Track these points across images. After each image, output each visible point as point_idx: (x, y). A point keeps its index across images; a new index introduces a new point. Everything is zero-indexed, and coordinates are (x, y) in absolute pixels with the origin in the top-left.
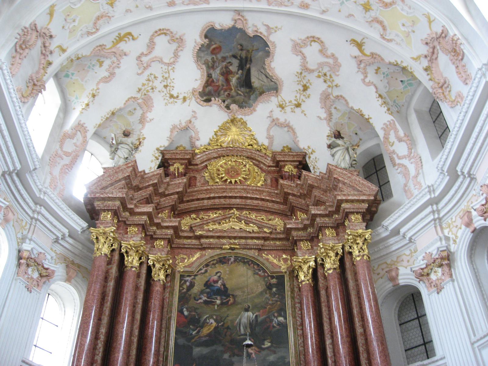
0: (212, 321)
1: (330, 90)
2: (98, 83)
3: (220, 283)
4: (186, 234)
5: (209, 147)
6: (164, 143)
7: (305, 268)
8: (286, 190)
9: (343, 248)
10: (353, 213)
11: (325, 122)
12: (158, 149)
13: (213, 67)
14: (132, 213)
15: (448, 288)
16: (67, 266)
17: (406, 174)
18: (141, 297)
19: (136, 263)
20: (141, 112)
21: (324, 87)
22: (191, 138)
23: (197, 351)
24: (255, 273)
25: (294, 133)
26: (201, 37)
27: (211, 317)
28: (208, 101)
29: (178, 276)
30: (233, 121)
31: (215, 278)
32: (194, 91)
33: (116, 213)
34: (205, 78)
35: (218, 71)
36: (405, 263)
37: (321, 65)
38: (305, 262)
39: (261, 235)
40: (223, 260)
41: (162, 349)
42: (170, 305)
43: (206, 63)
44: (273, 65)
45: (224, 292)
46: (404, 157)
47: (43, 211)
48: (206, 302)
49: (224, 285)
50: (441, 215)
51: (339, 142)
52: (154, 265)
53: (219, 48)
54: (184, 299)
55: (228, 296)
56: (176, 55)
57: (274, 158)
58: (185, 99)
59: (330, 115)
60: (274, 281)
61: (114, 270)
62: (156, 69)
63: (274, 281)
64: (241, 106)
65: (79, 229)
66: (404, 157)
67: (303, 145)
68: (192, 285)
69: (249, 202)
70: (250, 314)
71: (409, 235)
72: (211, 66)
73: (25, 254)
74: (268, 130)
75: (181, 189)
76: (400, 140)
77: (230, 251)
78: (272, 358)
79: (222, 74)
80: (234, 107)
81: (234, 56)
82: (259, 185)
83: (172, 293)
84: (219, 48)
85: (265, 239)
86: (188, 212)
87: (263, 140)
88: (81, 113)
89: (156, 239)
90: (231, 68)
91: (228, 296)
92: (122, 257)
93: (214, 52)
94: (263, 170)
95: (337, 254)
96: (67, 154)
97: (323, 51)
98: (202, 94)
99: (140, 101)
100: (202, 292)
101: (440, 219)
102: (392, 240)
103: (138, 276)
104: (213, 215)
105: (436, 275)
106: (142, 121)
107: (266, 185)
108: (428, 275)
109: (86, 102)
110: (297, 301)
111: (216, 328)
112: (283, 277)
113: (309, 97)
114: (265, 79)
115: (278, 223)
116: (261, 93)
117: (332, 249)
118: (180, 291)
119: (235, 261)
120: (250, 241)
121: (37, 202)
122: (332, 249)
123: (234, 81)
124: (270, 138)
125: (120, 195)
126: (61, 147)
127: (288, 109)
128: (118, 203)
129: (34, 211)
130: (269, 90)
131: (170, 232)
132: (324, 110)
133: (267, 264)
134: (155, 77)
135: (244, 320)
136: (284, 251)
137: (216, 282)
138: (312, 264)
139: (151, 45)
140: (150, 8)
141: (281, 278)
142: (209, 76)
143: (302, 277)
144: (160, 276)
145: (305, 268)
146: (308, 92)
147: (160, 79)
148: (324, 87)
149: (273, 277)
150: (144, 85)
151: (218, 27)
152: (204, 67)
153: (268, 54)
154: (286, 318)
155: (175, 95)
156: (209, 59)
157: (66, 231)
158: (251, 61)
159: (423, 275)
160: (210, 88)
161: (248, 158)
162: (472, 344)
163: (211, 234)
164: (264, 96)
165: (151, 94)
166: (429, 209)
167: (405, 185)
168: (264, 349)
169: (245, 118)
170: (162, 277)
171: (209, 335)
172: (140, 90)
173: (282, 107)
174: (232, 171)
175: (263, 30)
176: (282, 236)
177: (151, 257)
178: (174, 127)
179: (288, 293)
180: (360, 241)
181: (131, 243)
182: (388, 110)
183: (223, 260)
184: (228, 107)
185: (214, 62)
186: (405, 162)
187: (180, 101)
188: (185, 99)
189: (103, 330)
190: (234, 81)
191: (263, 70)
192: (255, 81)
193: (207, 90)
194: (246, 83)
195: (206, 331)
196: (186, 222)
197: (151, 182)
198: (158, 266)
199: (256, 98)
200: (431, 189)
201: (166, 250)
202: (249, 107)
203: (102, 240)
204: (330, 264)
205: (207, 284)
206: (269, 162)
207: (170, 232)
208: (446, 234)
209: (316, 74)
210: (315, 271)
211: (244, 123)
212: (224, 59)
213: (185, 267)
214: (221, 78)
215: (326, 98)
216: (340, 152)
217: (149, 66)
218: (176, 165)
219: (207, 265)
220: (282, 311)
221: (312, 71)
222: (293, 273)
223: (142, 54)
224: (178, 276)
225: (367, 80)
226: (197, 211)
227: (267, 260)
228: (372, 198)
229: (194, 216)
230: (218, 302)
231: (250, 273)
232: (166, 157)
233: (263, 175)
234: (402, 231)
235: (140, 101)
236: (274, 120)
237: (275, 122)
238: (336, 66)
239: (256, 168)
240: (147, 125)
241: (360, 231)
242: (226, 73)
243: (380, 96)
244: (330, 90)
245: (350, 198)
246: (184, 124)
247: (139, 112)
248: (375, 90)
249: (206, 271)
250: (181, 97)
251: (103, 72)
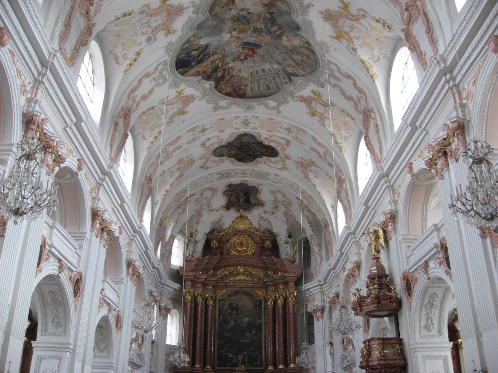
0: (232, 321)
1: (288, 211)
2: (178, 216)
3: (235, 304)
4: (220, 282)
5: (230, 231)
6: (208, 230)
7: (271, 300)
8: (265, 261)
9: (286, 295)
10: (290, 281)
11: (285, 223)
12: (205, 234)
13: (231, 196)
14: (198, 278)
15: (321, 320)
16: (173, 303)
17: (317, 261)
18: (204, 313)
19: (201, 301)
20: (197, 219)
21: (285, 209)
22: (220, 225)
23: (226, 335)
24: (250, 300)
25: (271, 225)
26: (225, 187)
27: (232, 320)
28: (230, 209)
29: (217, 301)
30: (241, 217)
31: (233, 302)
32: (222, 206)
33: (192, 281)
34: (227, 201)
35: (234, 197)
36: (310, 302)
37: (284, 201)
38: (271, 297)
39: (253, 282)
40: (236, 293)
41: (213, 333)
42: (215, 315)
43: (228, 195)
44: (260, 196)
45: (237, 309)
46: (316, 253)
47: (166, 287)
48: (230, 313)
49: (237, 305)
50: (324, 290)
51: (290, 240)
52: (208, 298)
53: (234, 190)
54: (221, 311)
55: (238, 310)
56: (213, 195)
57: (260, 237)
58: (217, 210)
59: (288, 220)
60: (258, 303)
61: (193, 306)
62: (204, 202)
63: (258, 303)
64: (245, 210)
65: (177, 288)
66: (316, 253)
67: (275, 231)
68: (224, 305)
69: (248, 262)
70: (247, 318)
71: (313, 293)
72: (229, 196)
73: (162, 308)
74: (259, 221)
75: (217, 261)
76: (316, 245)
77: (239, 289)
78: (255, 337)
79: (236, 198)
80: (241, 210)
81: (242, 192)
82: (253, 251)
83: (215, 308)
84: (234, 190)
85: (254, 283)
86: (220, 268)
87: (256, 225)
88: (172, 231)
89: (208, 285)
90: (240, 196)
91: (238, 310)
92: (195, 298)
93: (231, 191)
94: (256, 243)
95: (283, 297)
96: (167, 251)
97: (284, 196)
98: (225, 207)
99: (196, 215)
100: (228, 309)
101: (323, 291)
102: (307, 292)
103: (202, 305)
104: (232, 269)
105: (319, 314)
106: (198, 223)
107: (256, 250)
108: (316, 312)
109: (173, 225)
110: (267, 312)
111: (234, 325)
112: (261, 302)
113: (278, 211)
114: (257, 200)
115: (261, 274)
116: (255, 206)
117: (281, 295)
118: (219, 308)
119: (242, 293)
120: (248, 284)
121: (163, 284)
122: (281, 295)
123: (241, 200)
124: (260, 225)
125: (193, 274)
126: (165, 249)
127: (268, 214)
128: (193, 277)
129: (132, 236)
130: (259, 205)
131: (214, 282)
132: (285, 218)
133: (255, 294)
134: (203, 205)
135: (245, 321)
136: (263, 288)
137: (233, 304)
138: (274, 299)
139: (202, 194)
140: (202, 185)
141: (260, 302)
142: (229, 199)
143: (269, 303)
144: (211, 303)
145: (271, 300)
146: (278, 209)
147: (206, 204)
148: (285, 209)
149: (257, 302)
150: (198, 209)
151: (233, 183)
152: (227, 197)
153: (258, 192)
154: (262, 321)
155: (213, 209)
156: (229, 193)
157: (173, 290)
158: (250, 193)
159: (315, 311)
160: (230, 204)
161: (248, 235)
162: (324, 344)
163: (231, 282)
164: (255, 207)
165: (201, 211)
166: (319, 287)
167: (316, 267)
168: (252, 334)
169: (247, 215)
170: (211, 302)
171: (231, 327)
172: (196, 211)
173: (265, 212)
174: (241, 244)
175: (256, 185)
176: (262, 282)
177: (206, 295)
178: (213, 222)
179: (263, 310)
180: (292, 295)
181: (199, 292)
182: (312, 229)
183: (236, 293)
184: (239, 211)
185: (231, 194)
186: (316, 255)
187: (215, 212)
188: (217, 210)
189: (192, 331)
190: (241, 200)
191: (255, 197)
192: (252, 200)
193: (228, 205)
194: (248, 201)
195: (230, 326)
196: (220, 273)
197: (205, 262)
198: (209, 299)
199: (253, 207)
200: (320, 281)
201: (212, 291)
202: (249, 210)
203: (188, 295)
204: (280, 301)
205: (230, 305)
206: (258, 239)
207: (214, 282)
208: (325, 299)
209: (281, 203)
210: (275, 301)
211: (246, 218)
212: (237, 193)
213: (220, 296)
214: (235, 199)
215: (285, 214)
216: (289, 247)
217: (200, 201)
218: (214, 241)
219: (230, 296)
220: (260, 318)
221: (280, 202)
222: (266, 301)
223: (198, 198)
224: (217, 301)
225: (304, 214)
226: (225, 267)
227: (256, 292)
228: (299, 276)
229: (223, 269)
230: (235, 313)
231: (248, 299)
232: (210, 237)
233: (255, 245)
234: (311, 290)
235: (196, 215)
236: (261, 217)
237: (262, 218)
238: (290, 203)
239: (252, 241)
240: (200, 225)
241: (292, 291)
242: (238, 198)
243: (309, 222)
244: (288, 211)
245: (290, 275)
246: (217, 220)
247: (196, 219)
248: (307, 219)
249: (229, 299)
250: (216, 209)
251: (180, 211)
